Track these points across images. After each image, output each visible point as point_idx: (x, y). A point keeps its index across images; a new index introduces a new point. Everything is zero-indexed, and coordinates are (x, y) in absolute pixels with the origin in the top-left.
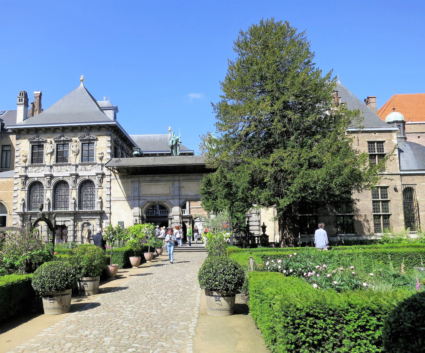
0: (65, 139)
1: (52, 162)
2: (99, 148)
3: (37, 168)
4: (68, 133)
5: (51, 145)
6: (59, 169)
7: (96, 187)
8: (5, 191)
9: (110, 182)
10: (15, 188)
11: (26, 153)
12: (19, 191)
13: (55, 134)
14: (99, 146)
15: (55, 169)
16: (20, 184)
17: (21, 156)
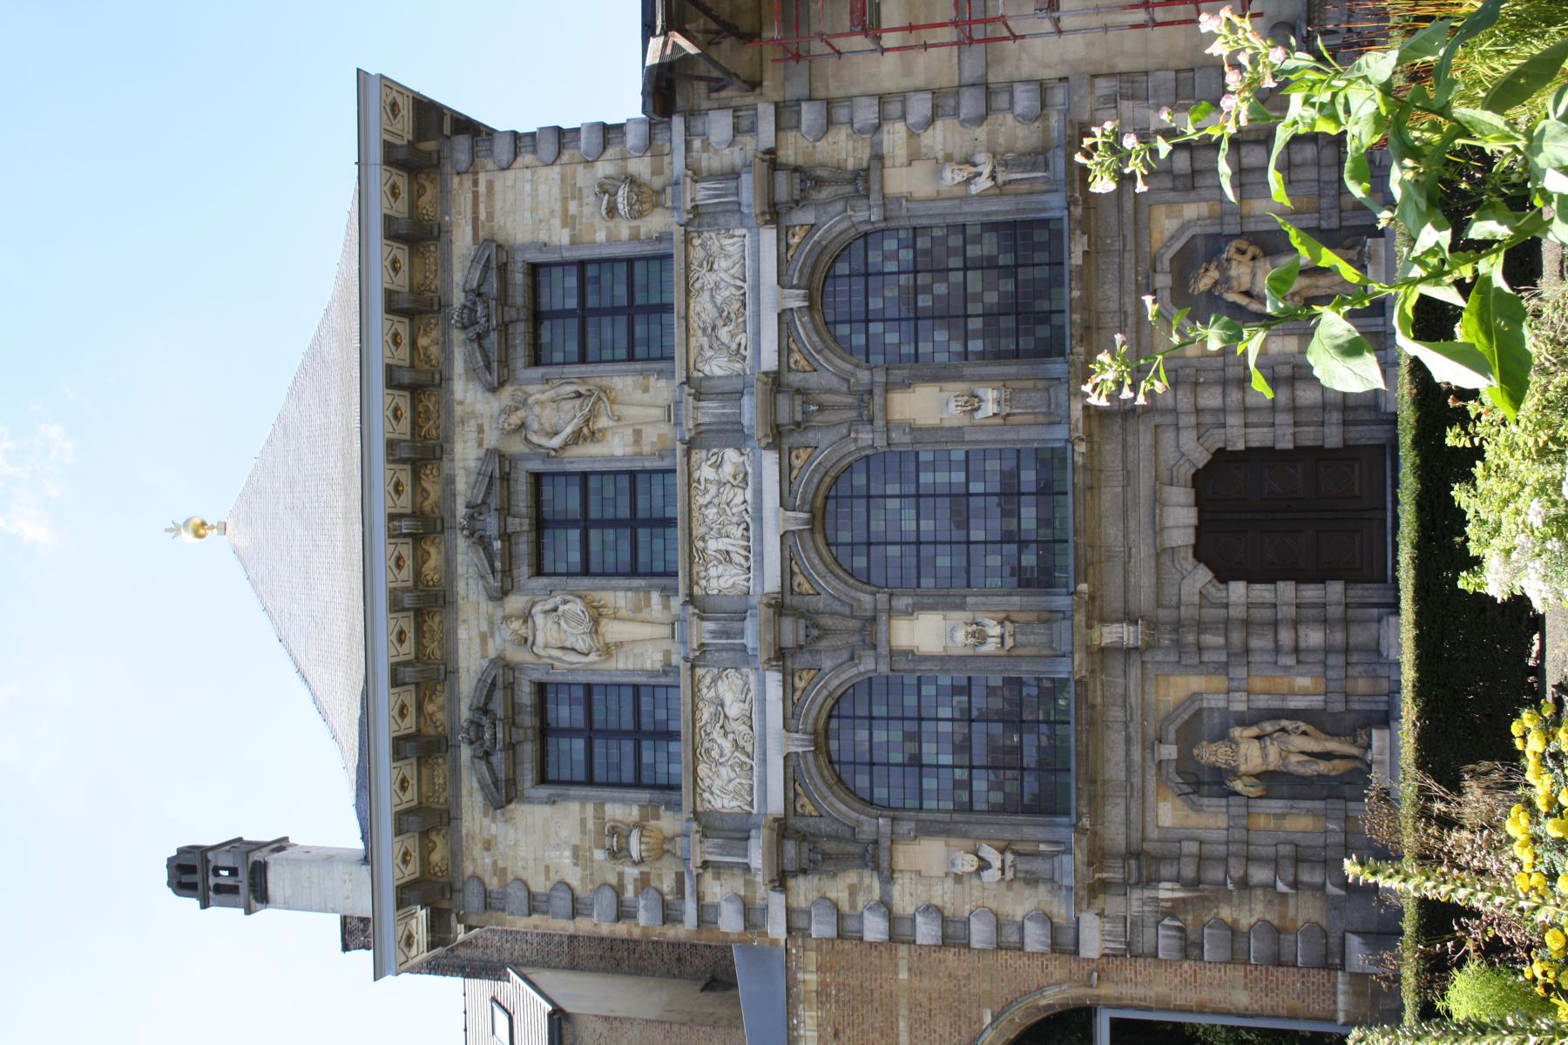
0: (494, 502)
1: (666, 607)
2: (568, 221)
3: (717, 734)
4: (451, 480)
5: (540, 620)
6: (723, 544)
7: (867, 214)
8: (893, 1026)
9: (829, 103)
10: (875, 929)
11: (600, 832)
12: (905, 898)
13: (461, 586)
14: (556, 222)
15: (724, 583)
16: (838, 889)
17: (621, 875)
